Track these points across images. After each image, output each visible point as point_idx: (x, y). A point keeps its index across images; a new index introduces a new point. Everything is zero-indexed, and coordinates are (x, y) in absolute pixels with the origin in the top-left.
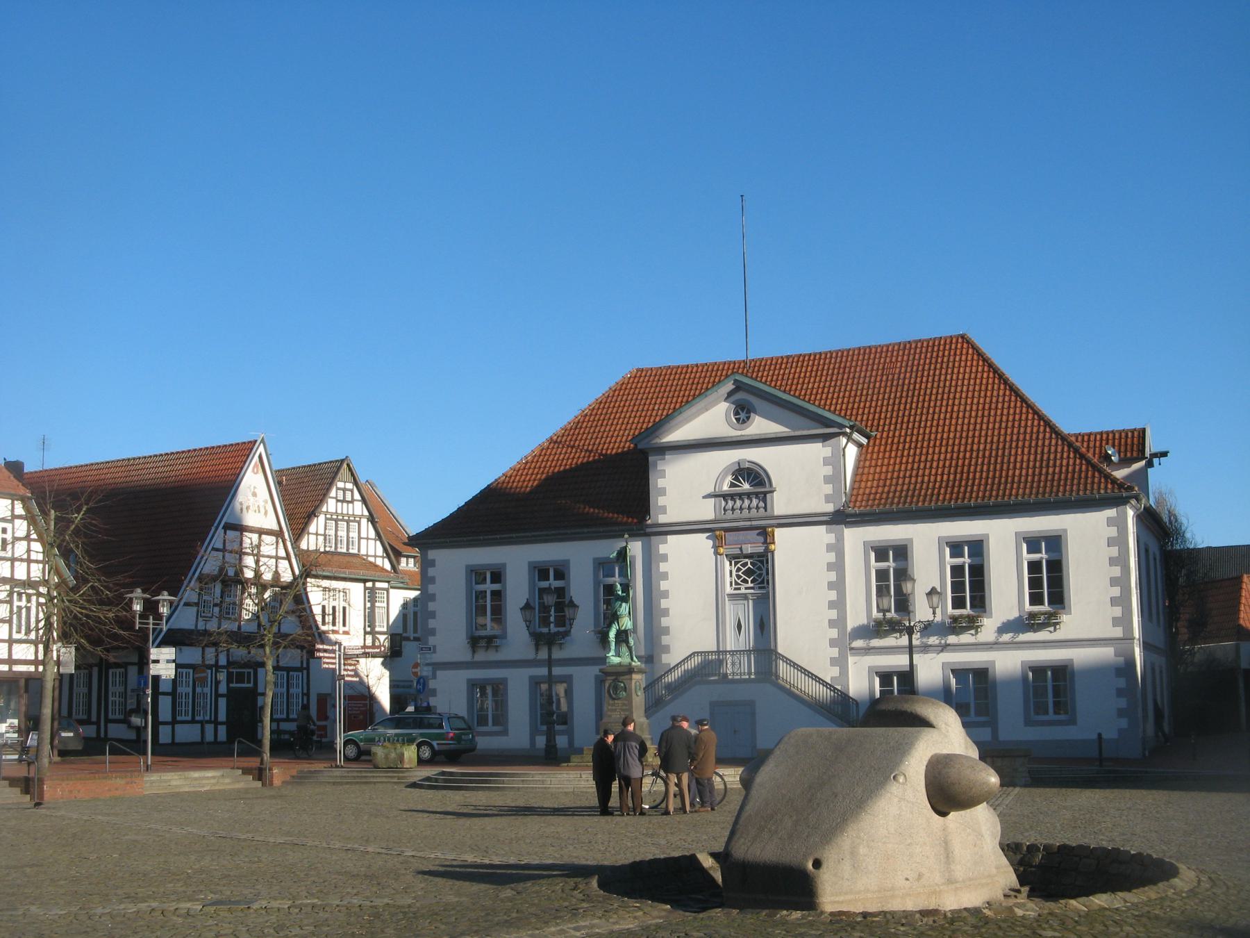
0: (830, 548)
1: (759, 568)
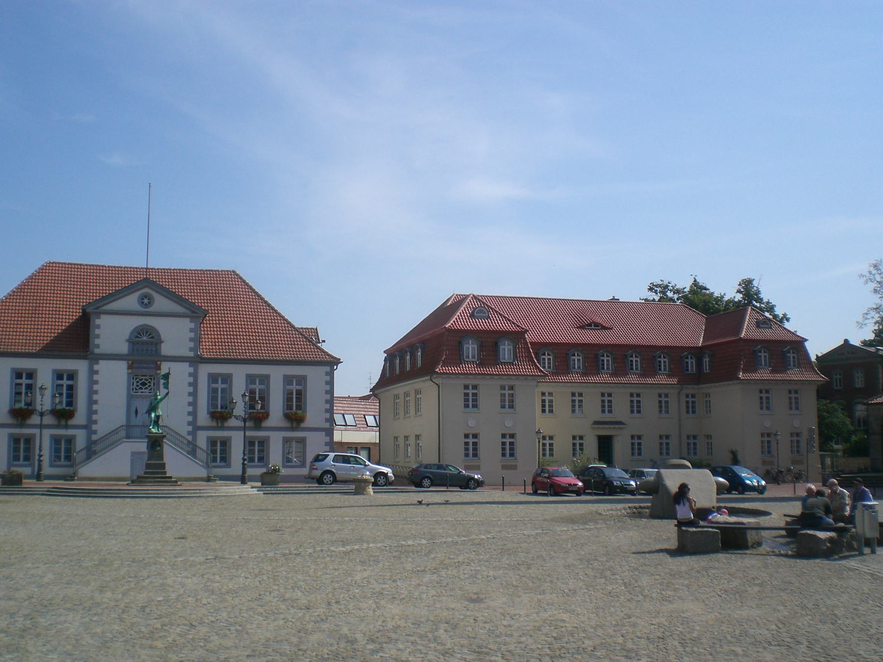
0: (190, 375)
1: (150, 382)
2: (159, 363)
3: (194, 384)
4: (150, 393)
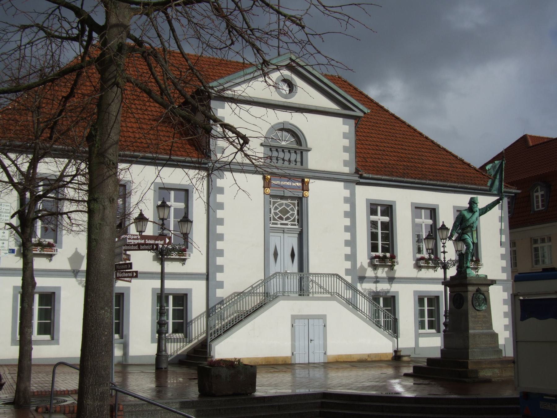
0: (346, 200)
2: (306, 180)
3: (351, 214)
4: (292, 225)
